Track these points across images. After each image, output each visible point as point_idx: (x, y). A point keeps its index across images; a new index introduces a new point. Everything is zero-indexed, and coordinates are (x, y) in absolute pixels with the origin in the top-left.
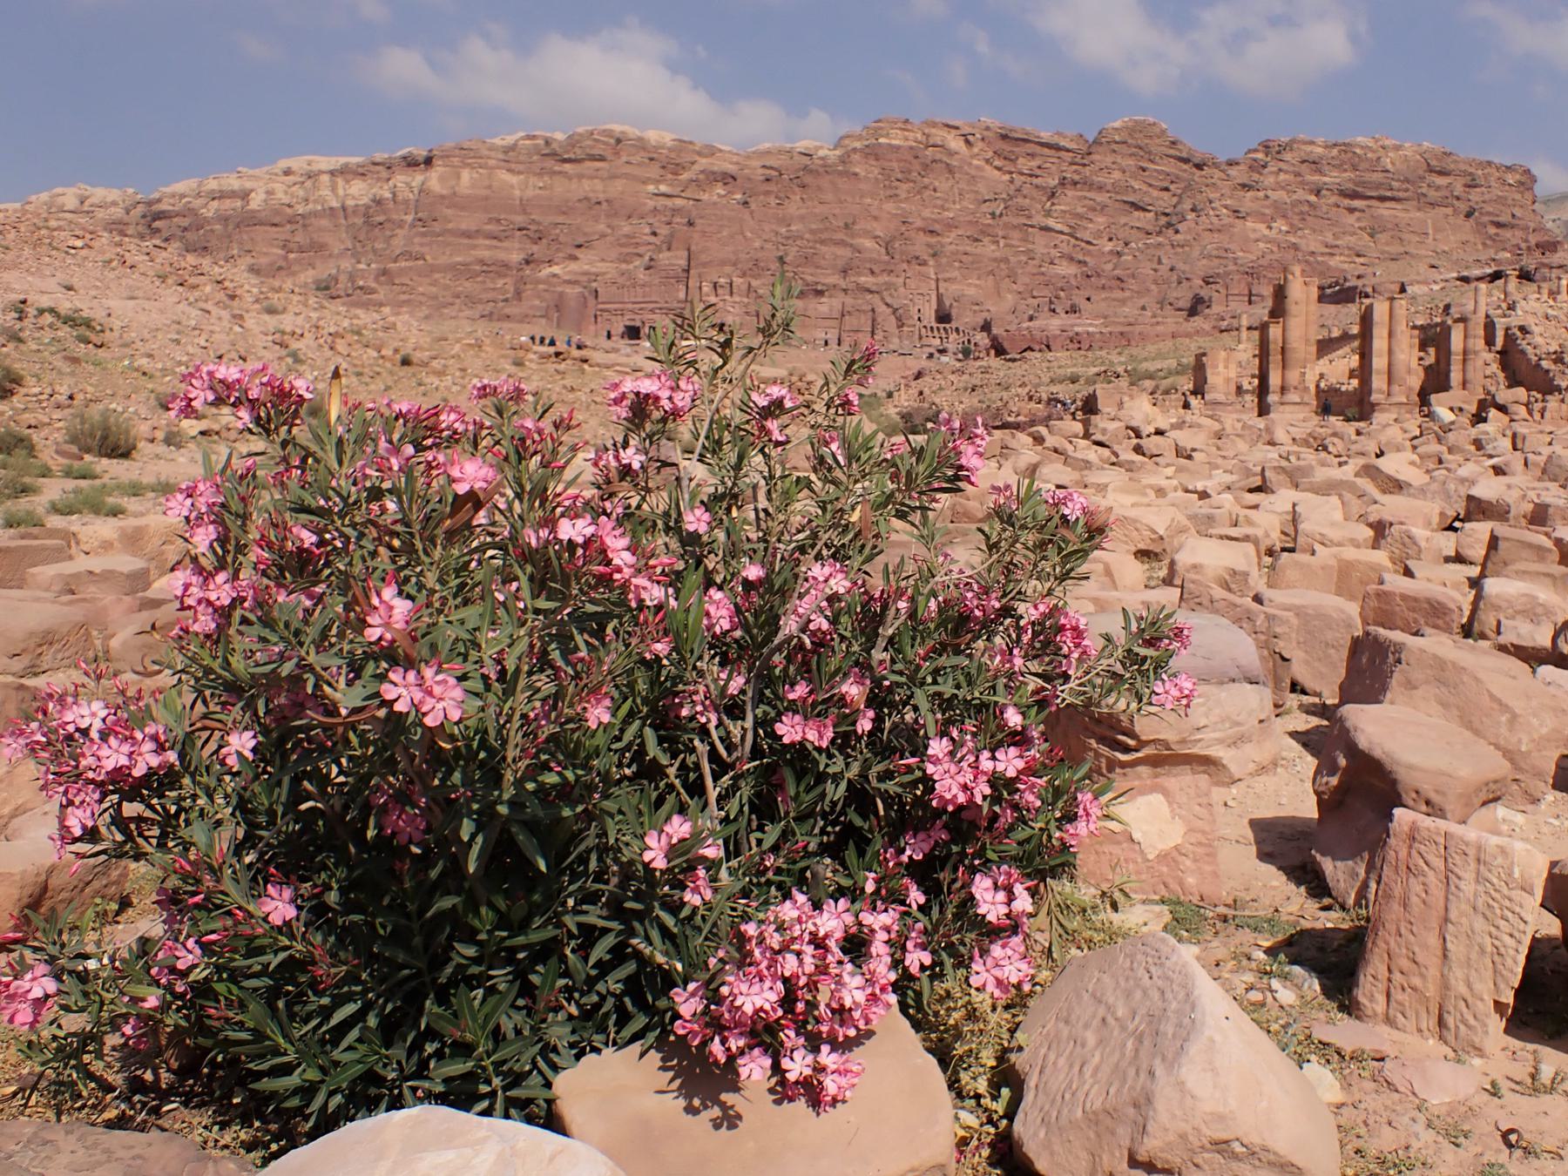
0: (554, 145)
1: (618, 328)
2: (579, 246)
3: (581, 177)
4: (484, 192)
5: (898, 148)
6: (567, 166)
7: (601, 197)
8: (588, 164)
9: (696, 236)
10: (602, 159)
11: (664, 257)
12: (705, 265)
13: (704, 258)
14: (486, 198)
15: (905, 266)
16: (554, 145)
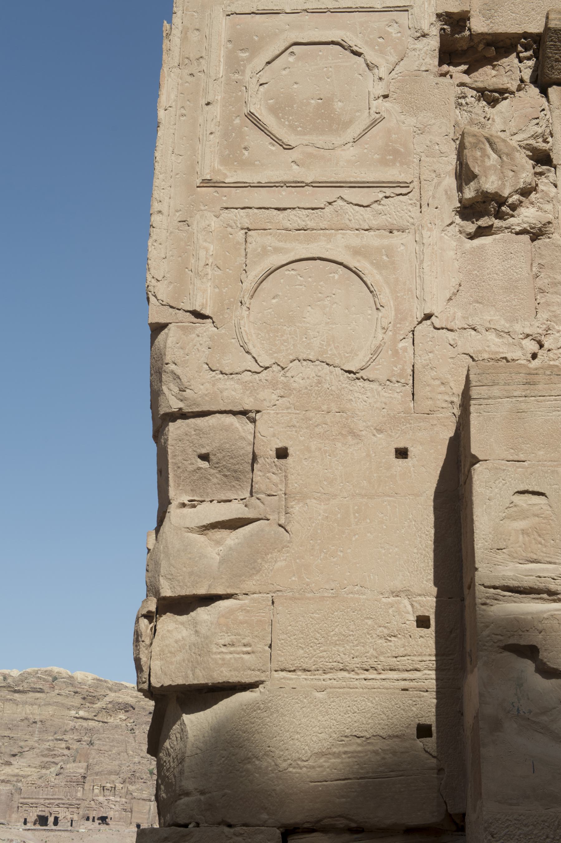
0: (10, 680)
1: (32, 817)
2: (14, 755)
3: (26, 703)
6: (17, 695)
7: (38, 718)
8: (31, 694)
9: (93, 752)
10: (41, 691)
11: (71, 767)
12: (97, 774)
13: (97, 768)
16: (10, 680)
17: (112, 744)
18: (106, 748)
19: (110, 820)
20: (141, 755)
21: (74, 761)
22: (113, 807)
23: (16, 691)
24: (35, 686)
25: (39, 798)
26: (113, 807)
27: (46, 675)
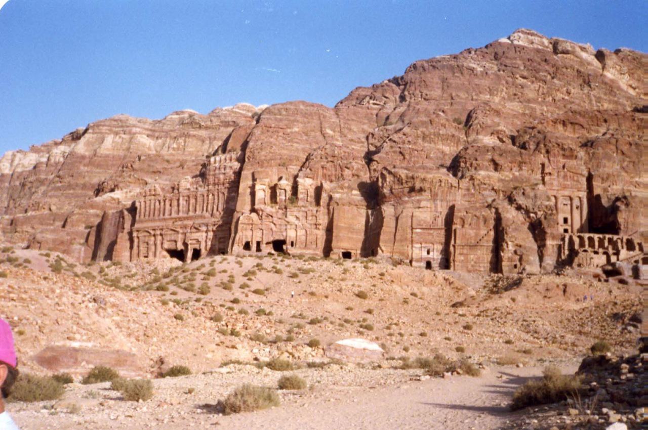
4: (122, 153)
5: (523, 48)
6: (203, 133)
9: (257, 132)
12: (261, 164)
14: (125, 157)
15: (541, 158)
17: (292, 118)
18: (282, 125)
19: (289, 247)
20: (349, 136)
21: (224, 151)
22: (297, 222)
23: (200, 127)
24: (226, 120)
25: (165, 220)
26: (297, 222)
27: (243, 110)
